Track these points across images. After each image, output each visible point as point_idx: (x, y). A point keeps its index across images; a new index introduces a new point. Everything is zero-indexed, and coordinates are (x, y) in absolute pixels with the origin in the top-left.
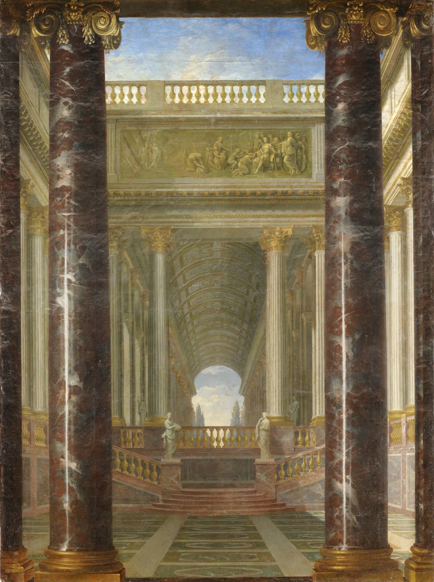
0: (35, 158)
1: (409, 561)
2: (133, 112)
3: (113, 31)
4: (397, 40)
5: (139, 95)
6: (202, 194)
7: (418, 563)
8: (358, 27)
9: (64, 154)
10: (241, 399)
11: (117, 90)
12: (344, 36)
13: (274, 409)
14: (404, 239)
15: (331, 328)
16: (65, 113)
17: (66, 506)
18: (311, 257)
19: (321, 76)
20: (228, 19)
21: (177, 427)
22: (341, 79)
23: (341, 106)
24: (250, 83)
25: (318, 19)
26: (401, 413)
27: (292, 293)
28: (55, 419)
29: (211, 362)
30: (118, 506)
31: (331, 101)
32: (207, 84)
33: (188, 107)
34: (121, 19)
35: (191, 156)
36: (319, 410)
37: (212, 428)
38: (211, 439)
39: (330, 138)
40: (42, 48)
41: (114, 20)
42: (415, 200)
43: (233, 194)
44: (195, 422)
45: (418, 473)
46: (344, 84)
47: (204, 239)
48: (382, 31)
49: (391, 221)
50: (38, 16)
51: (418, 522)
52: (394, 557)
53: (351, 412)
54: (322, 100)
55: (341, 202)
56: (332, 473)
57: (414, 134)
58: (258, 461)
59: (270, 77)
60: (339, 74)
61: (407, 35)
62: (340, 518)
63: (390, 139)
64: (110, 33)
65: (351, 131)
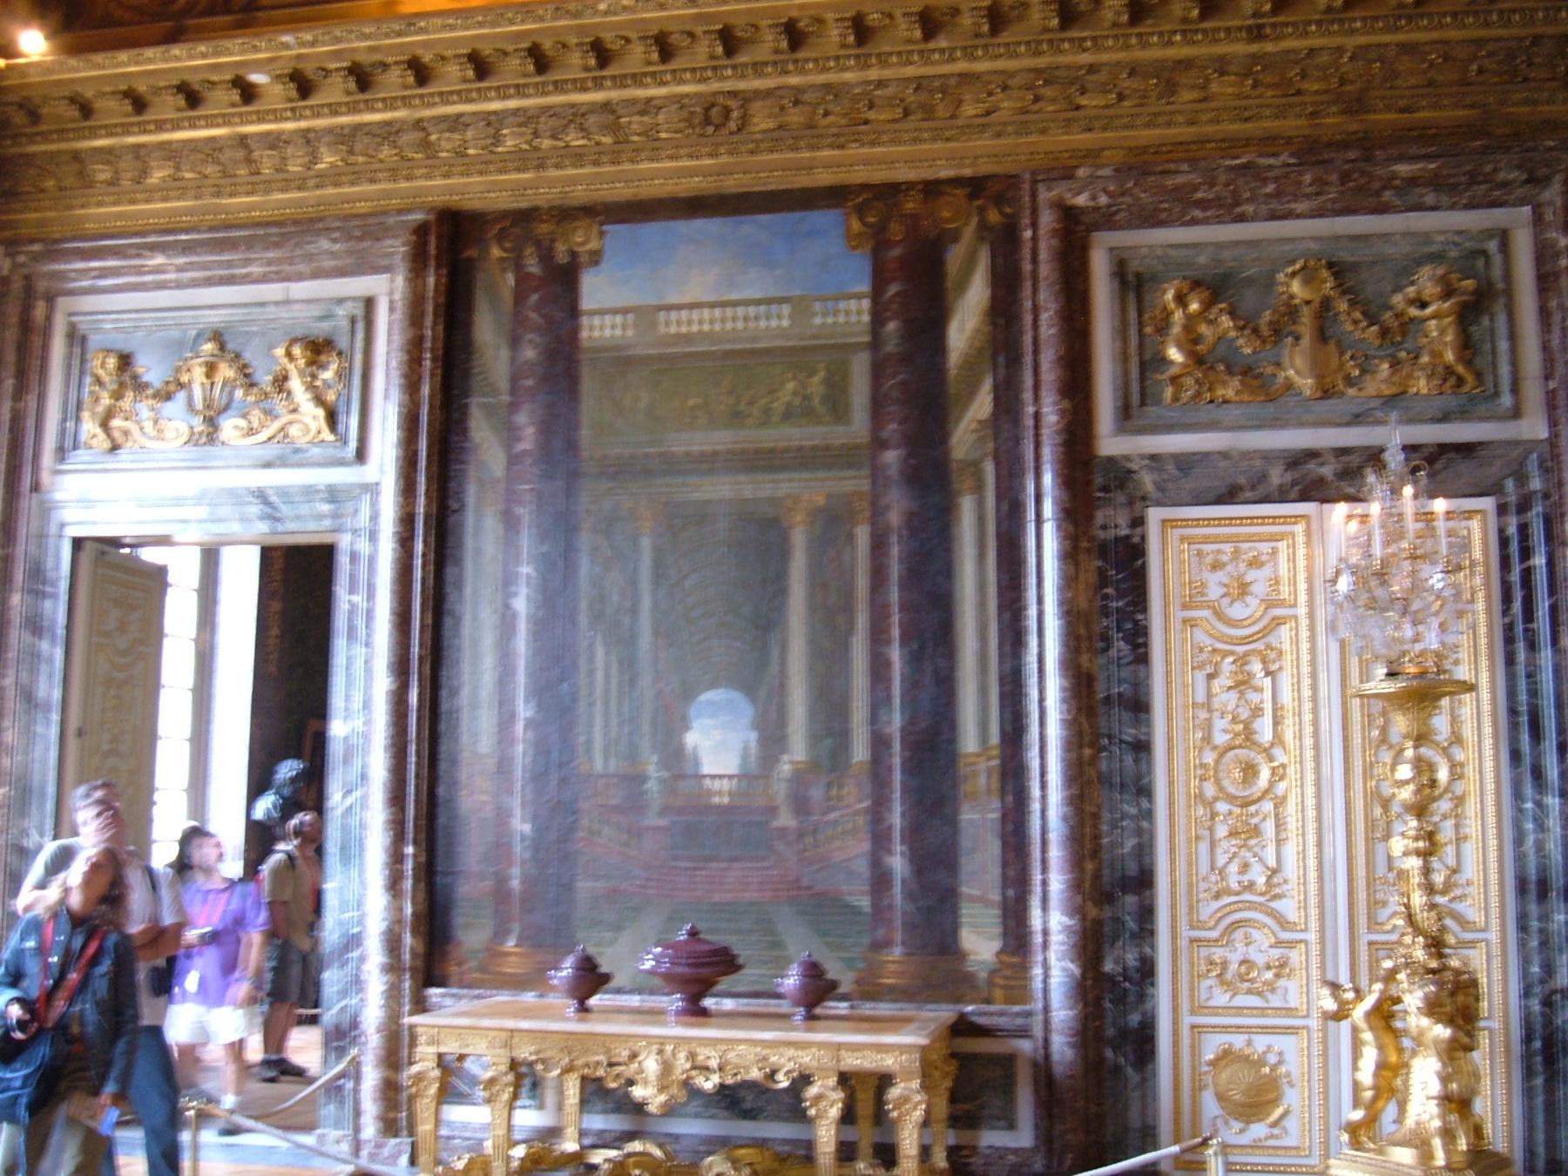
0: (490, 411)
1: (993, 973)
2: (617, 348)
3: (593, 245)
4: (969, 232)
5: (624, 327)
6: (702, 454)
7: (1007, 978)
8: (915, 217)
9: (527, 407)
10: (753, 736)
11: (596, 321)
12: (896, 230)
13: (798, 750)
14: (981, 505)
15: (878, 636)
16: (530, 354)
17: (515, 884)
18: (850, 538)
19: (865, 287)
20: (742, 218)
21: (665, 774)
22: (893, 289)
23: (892, 326)
24: (769, 301)
25: (861, 211)
26: (977, 755)
27: (824, 585)
28: (504, 766)
29: (713, 685)
30: (585, 887)
31: (878, 320)
32: (712, 305)
33: (687, 338)
34: (605, 228)
35: (691, 402)
36: (860, 751)
37: (713, 777)
38: (710, 793)
39: (877, 372)
40: (504, 270)
41: (595, 230)
42: (996, 449)
43: (743, 452)
44: (689, 770)
45: (1005, 844)
46: (897, 294)
47: (701, 515)
48: (948, 221)
49: (962, 482)
50: (502, 230)
51: (1005, 916)
52: (971, 967)
53: (907, 754)
54: (866, 318)
55: (892, 457)
56: (880, 840)
57: (995, 355)
58: (776, 823)
59: (797, 292)
60: (888, 283)
61: (983, 226)
62: (890, 907)
63: (961, 368)
64: (588, 247)
65: (905, 359)
